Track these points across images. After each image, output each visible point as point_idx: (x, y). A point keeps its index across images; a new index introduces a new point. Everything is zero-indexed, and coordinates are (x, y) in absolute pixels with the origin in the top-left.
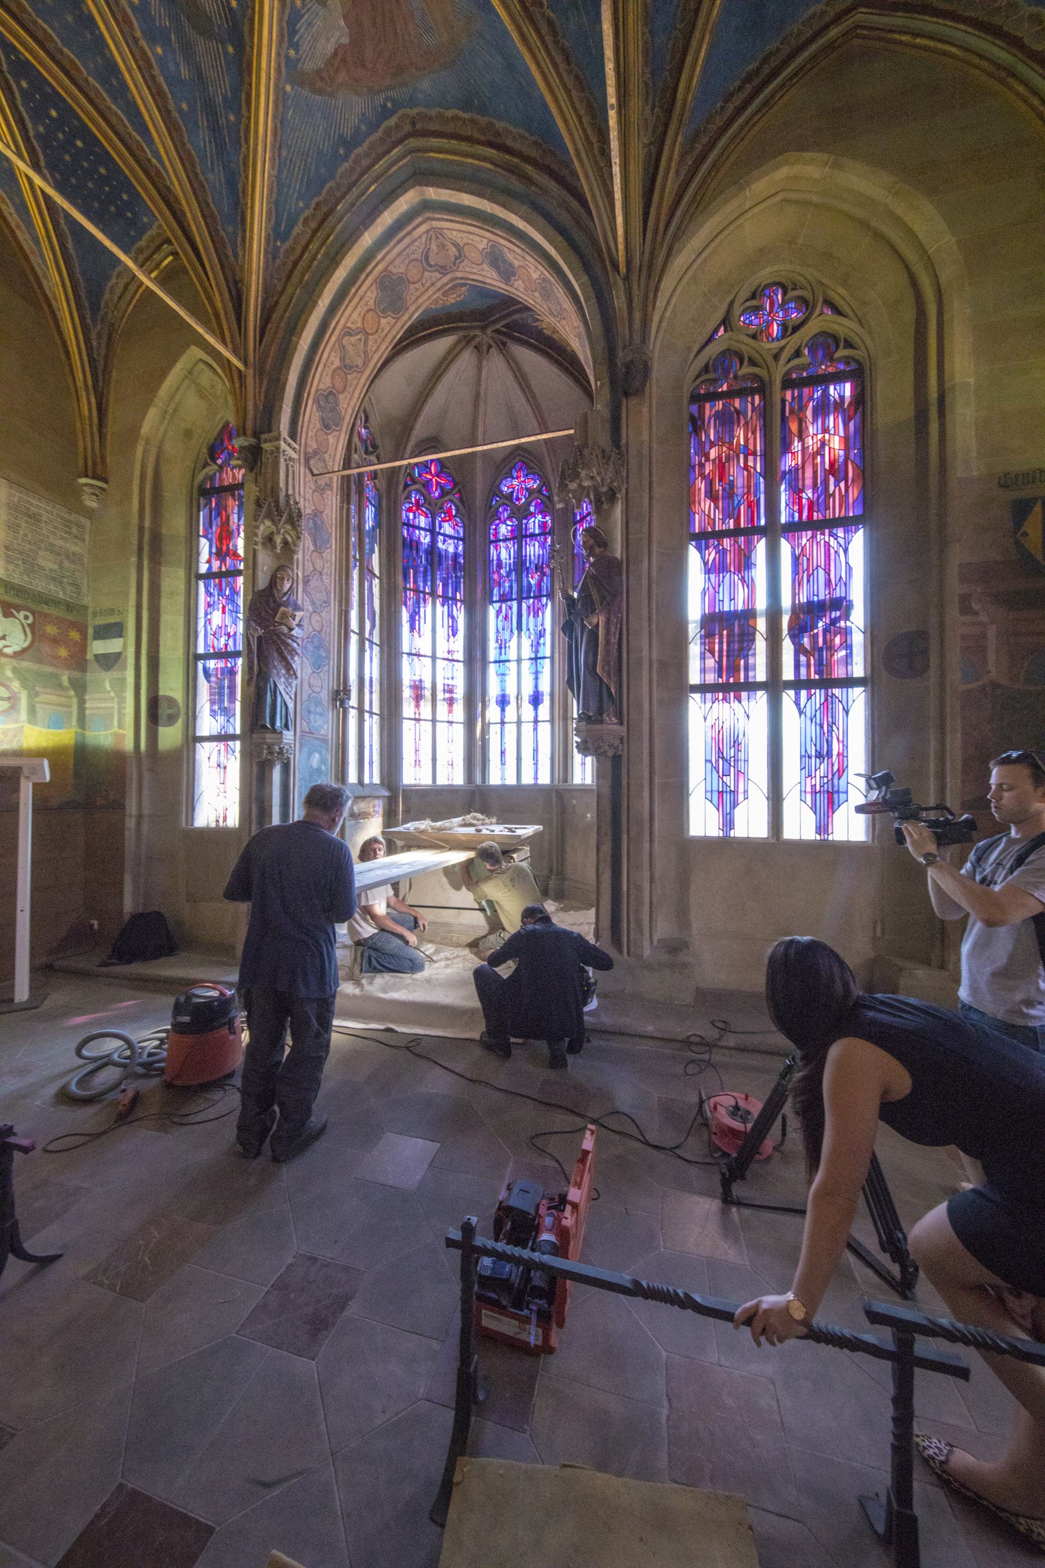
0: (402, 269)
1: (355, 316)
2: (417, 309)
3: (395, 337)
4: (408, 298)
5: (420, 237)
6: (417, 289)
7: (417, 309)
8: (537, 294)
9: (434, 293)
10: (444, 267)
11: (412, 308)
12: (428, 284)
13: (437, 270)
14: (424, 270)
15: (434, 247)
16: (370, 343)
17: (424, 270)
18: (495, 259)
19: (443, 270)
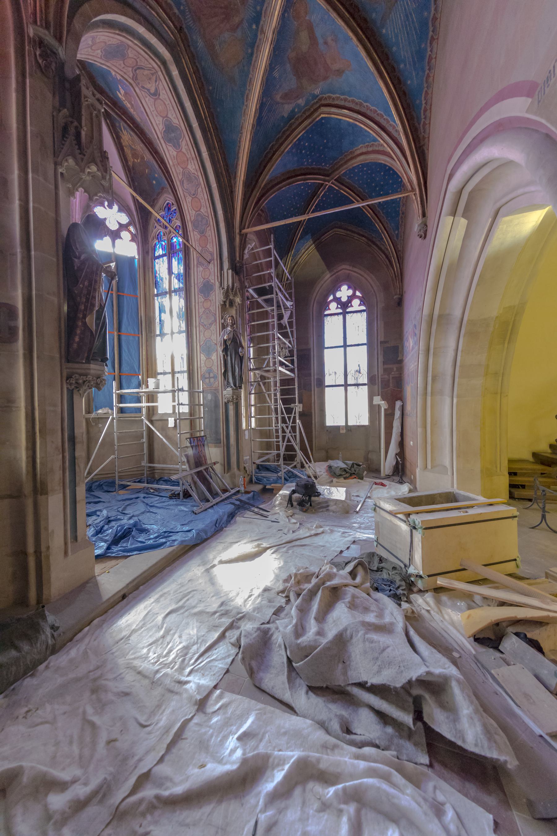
0: (130, 55)
1: (103, 37)
2: (108, 66)
3: (89, 59)
4: (114, 61)
5: (150, 64)
6: (120, 65)
7: (108, 66)
8: (182, 170)
9: (119, 74)
10: (136, 79)
11: (108, 64)
12: (125, 71)
13: (134, 75)
14: (133, 67)
15: (146, 72)
16: (86, 50)
17: (133, 67)
18: (169, 128)
19: (135, 78)
